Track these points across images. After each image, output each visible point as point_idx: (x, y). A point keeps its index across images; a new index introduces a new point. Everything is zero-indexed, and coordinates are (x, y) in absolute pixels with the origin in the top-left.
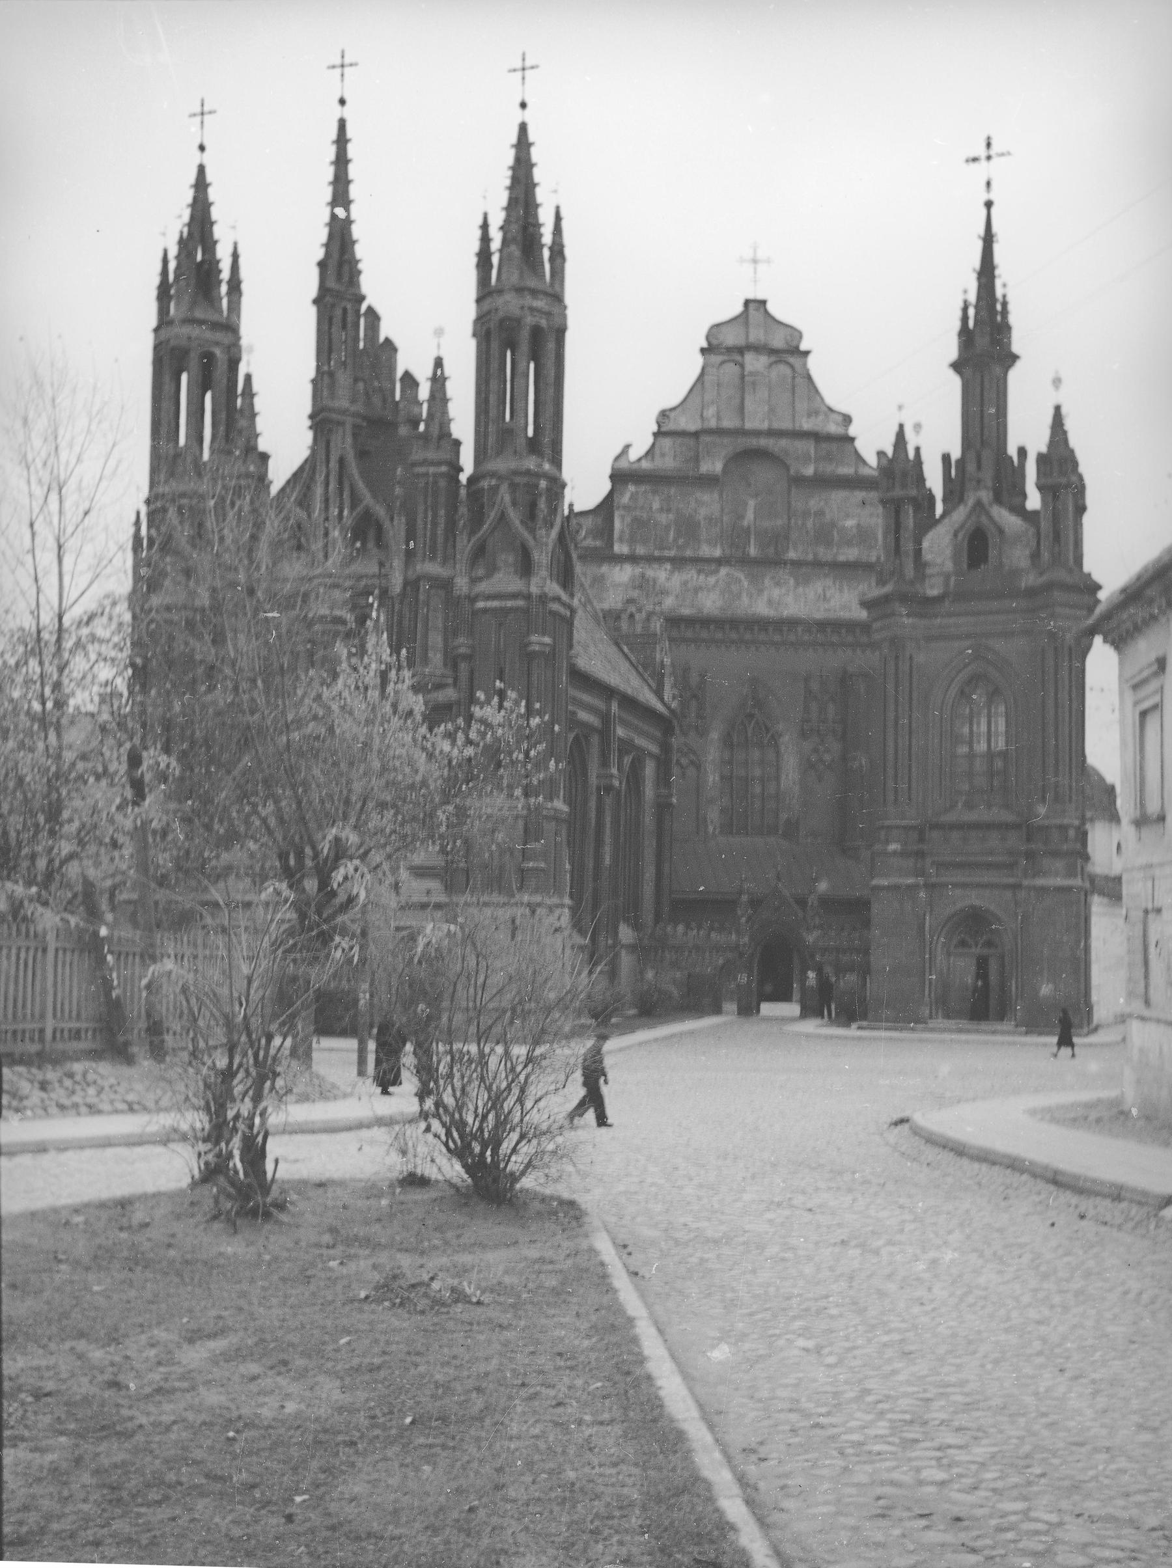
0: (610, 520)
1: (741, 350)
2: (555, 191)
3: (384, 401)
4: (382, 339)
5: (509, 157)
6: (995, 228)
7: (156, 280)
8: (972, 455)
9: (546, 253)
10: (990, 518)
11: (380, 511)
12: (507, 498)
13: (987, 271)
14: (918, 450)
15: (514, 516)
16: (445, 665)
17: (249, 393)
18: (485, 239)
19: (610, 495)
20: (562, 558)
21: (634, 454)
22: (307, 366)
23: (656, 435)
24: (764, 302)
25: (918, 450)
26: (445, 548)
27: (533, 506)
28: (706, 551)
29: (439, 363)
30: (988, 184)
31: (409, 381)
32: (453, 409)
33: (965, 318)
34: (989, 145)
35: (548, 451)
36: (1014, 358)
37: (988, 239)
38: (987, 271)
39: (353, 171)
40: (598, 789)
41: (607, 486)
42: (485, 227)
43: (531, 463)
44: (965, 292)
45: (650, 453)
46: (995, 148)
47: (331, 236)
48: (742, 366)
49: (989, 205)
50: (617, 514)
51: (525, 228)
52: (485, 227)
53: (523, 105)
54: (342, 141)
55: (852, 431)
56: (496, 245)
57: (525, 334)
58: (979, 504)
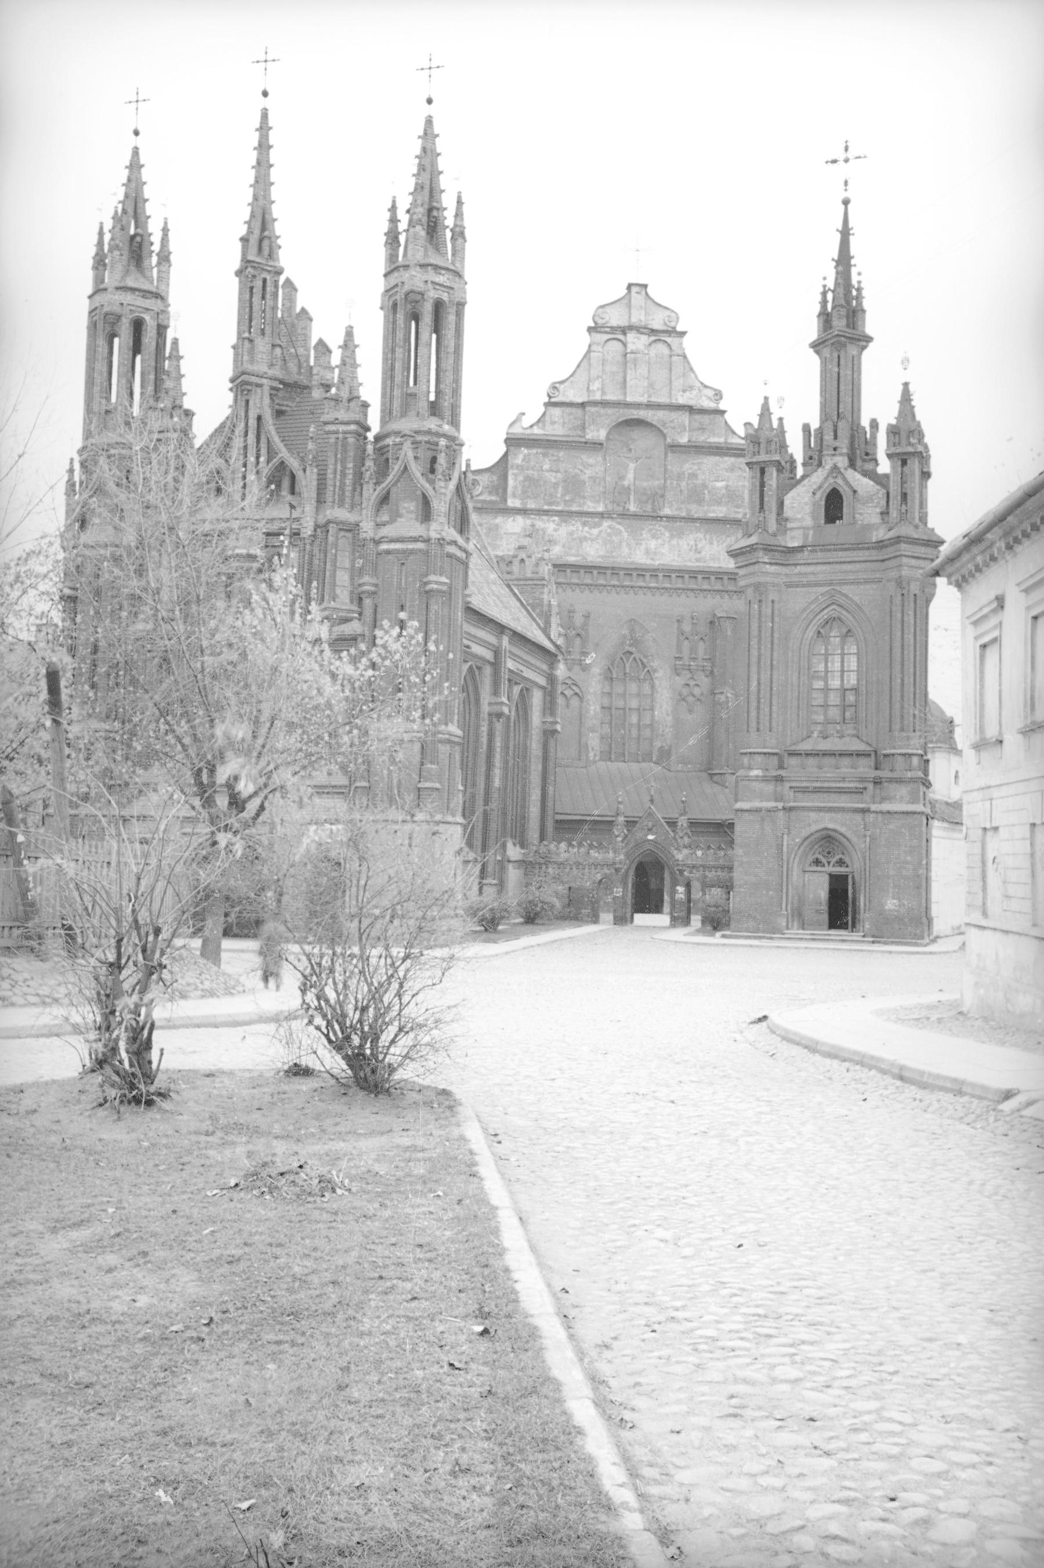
0: (505, 478)
1: (624, 330)
3: (300, 367)
4: (298, 310)
5: (417, 147)
7: (93, 251)
8: (829, 425)
10: (845, 479)
11: (294, 463)
12: (410, 454)
13: (844, 260)
14: (781, 419)
15: (416, 470)
16: (352, 602)
17: (176, 357)
18: (394, 220)
19: (506, 455)
20: (459, 508)
21: (526, 422)
22: (230, 334)
23: (547, 405)
24: (645, 286)
25: (781, 419)
26: (353, 497)
27: (434, 460)
28: (590, 506)
29: (349, 333)
30: (846, 183)
31: (323, 348)
32: (362, 374)
33: (824, 302)
34: (846, 149)
35: (447, 413)
36: (869, 339)
37: (845, 233)
38: (844, 260)
39: (274, 156)
42: (393, 209)
43: (432, 424)
47: (253, 215)
48: (625, 345)
49: (846, 202)
50: (510, 472)
51: (430, 210)
52: (393, 209)
53: (430, 101)
54: (264, 128)
55: (722, 406)
56: (403, 226)
58: (835, 467)
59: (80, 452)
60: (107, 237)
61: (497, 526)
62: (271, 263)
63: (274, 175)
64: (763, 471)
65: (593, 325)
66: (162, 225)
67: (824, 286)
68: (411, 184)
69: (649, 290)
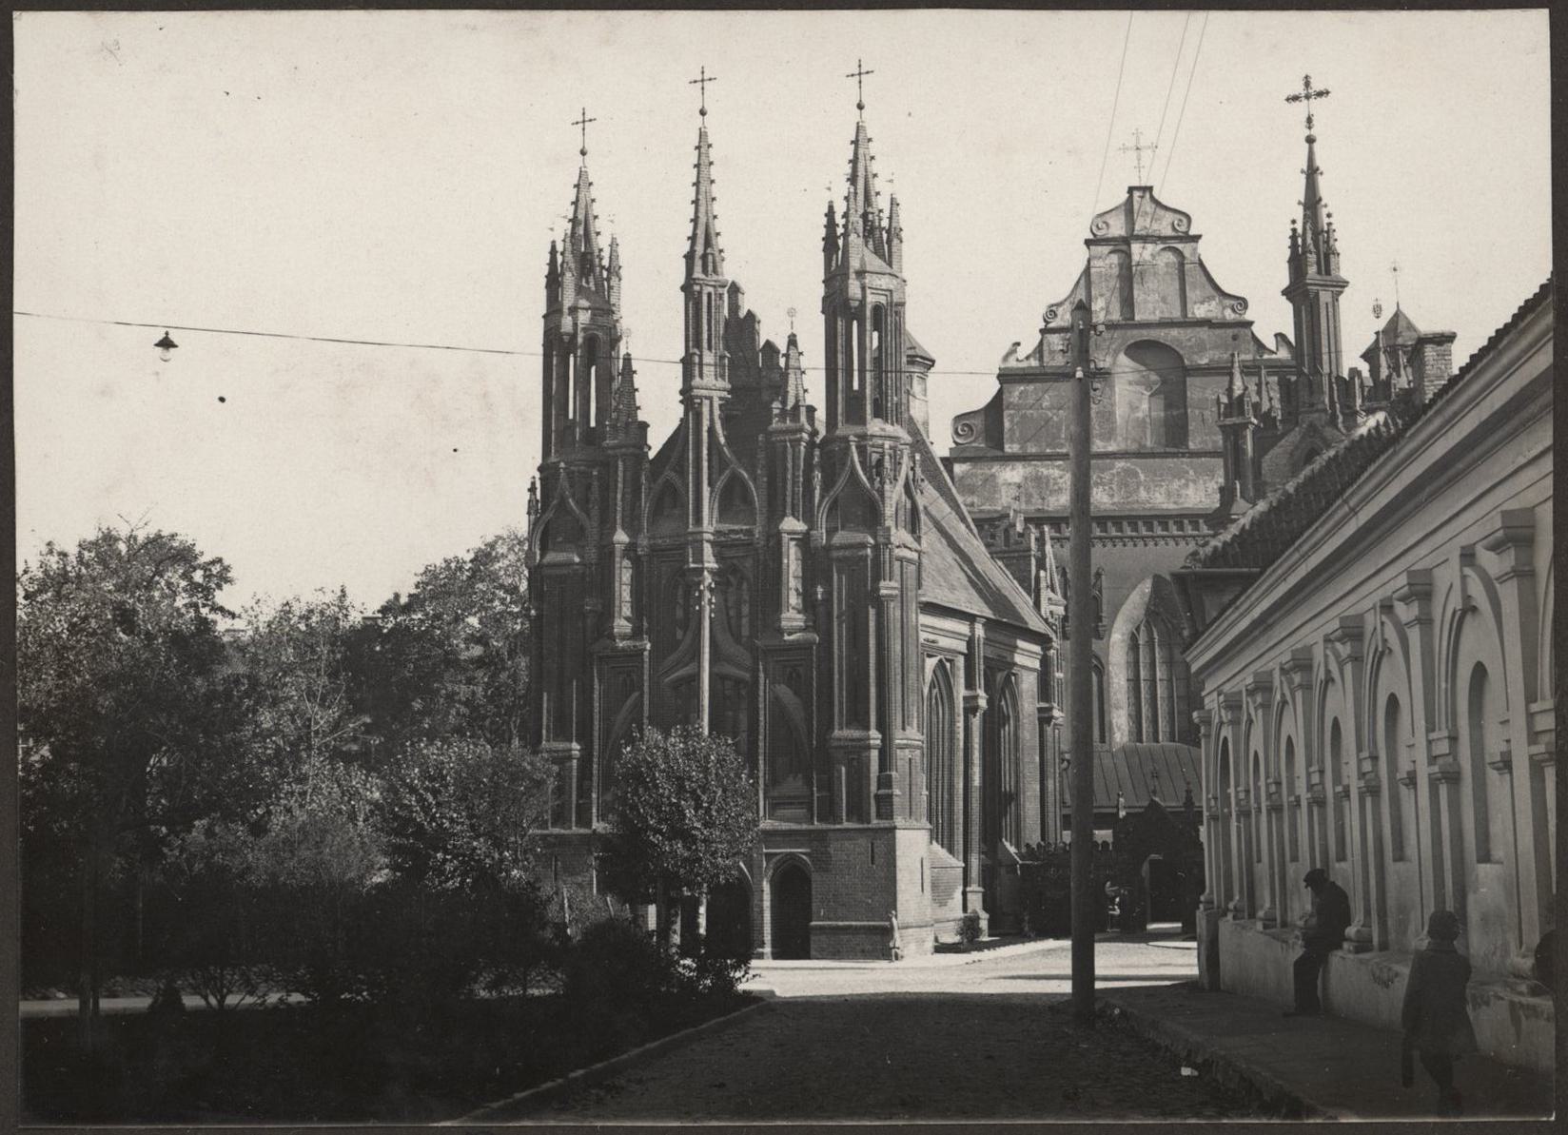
2: (891, 181)
6: (1319, 162)
7: (546, 270)
13: (1312, 202)
17: (628, 372)
19: (1000, 392)
20: (909, 506)
21: (1023, 352)
23: (1043, 332)
24: (1150, 189)
30: (1309, 120)
33: (1294, 246)
34: (1307, 84)
37: (1312, 172)
42: (830, 214)
44: (1294, 222)
45: (1039, 350)
48: (1129, 255)
49: (1310, 140)
50: (1006, 413)
54: (703, 145)
55: (1248, 316)
58: (1312, 426)
59: (540, 469)
65: (1092, 237)
67: (1294, 230)
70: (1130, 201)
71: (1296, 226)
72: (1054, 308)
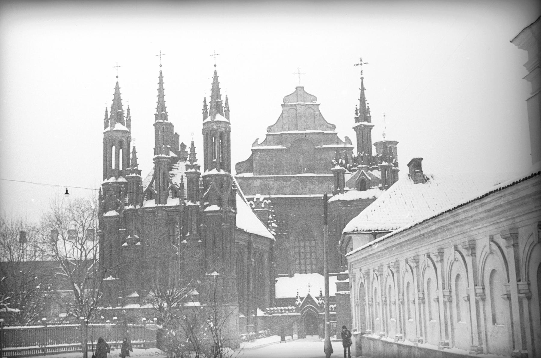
0: (252, 165)
4: (174, 133)
6: (364, 86)
9: (224, 109)
18: (205, 106)
21: (259, 142)
24: (303, 87)
27: (222, 185)
29: (193, 144)
30: (362, 72)
31: (184, 146)
34: (361, 60)
35: (226, 167)
37: (363, 89)
40: (248, 265)
41: (251, 153)
42: (205, 102)
44: (356, 105)
46: (363, 61)
49: (362, 78)
50: (254, 162)
52: (205, 102)
53: (215, 66)
55: (336, 131)
56: (208, 107)
57: (218, 134)
60: (109, 114)
61: (250, 184)
62: (165, 121)
63: (165, 92)
64: (338, 174)
65: (283, 104)
66: (127, 108)
67: (356, 108)
68: (210, 93)
69: (304, 88)
70: (297, 90)
71: (357, 107)
72: (271, 127)
